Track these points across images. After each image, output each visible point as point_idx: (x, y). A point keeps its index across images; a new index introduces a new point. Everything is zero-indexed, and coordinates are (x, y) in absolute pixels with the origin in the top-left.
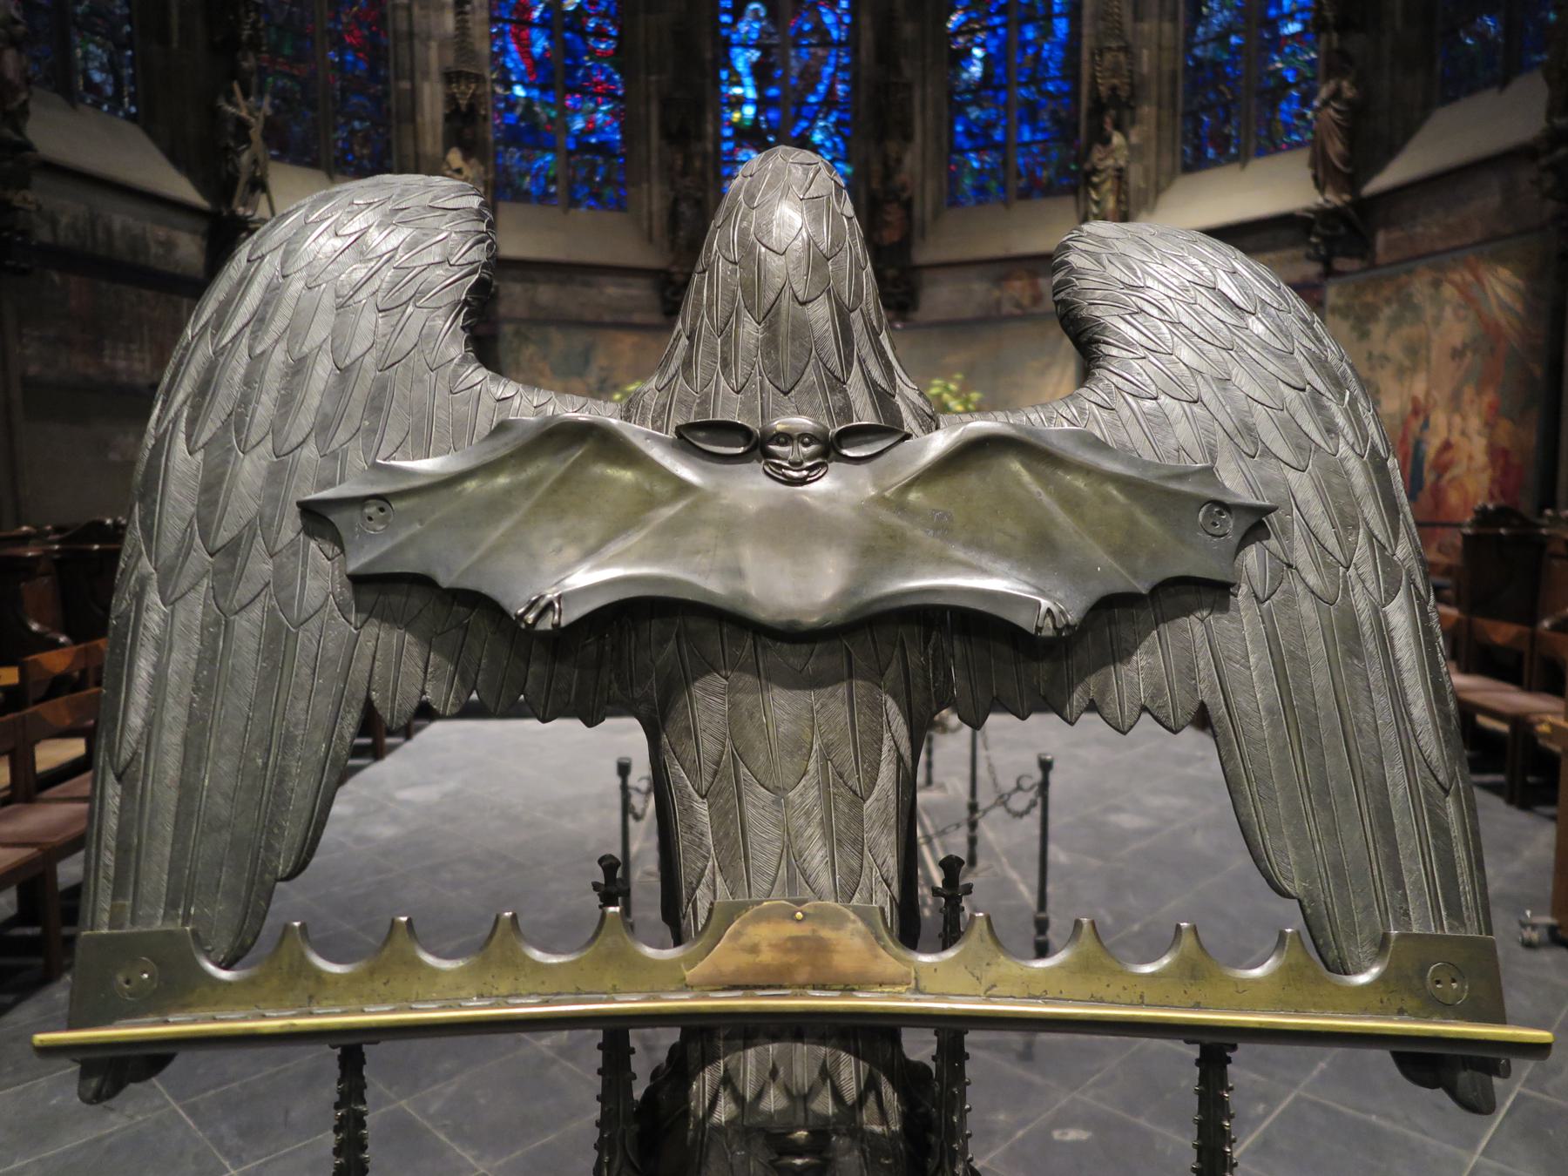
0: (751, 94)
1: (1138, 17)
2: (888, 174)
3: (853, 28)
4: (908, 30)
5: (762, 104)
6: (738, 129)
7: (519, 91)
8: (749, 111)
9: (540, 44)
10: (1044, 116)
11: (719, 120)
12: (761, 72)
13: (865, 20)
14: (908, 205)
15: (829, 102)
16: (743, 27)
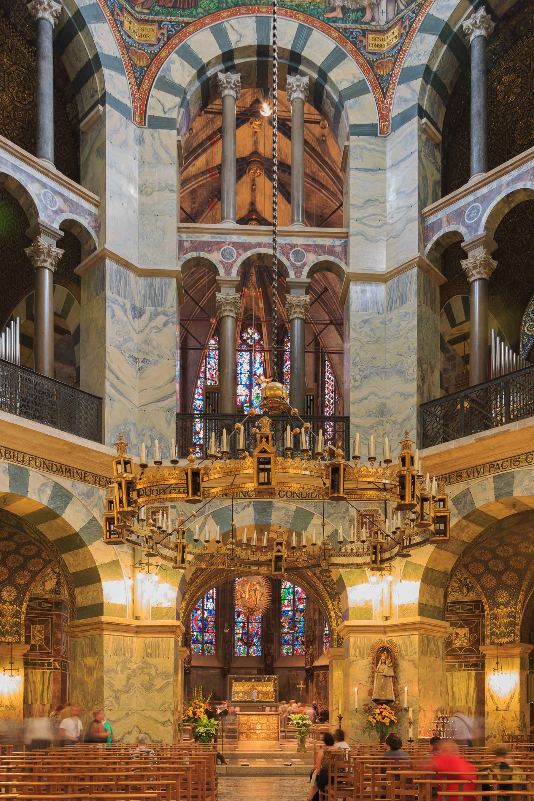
0: (241, 632)
1: (315, 625)
2: (268, 650)
3: (262, 619)
4: (273, 622)
5: (243, 634)
6: (238, 639)
7: (195, 633)
8: (240, 635)
9: (200, 624)
10: (299, 639)
11: (234, 637)
12: (243, 627)
13: (264, 619)
14: (272, 656)
15: (257, 634)
16: (240, 619)
